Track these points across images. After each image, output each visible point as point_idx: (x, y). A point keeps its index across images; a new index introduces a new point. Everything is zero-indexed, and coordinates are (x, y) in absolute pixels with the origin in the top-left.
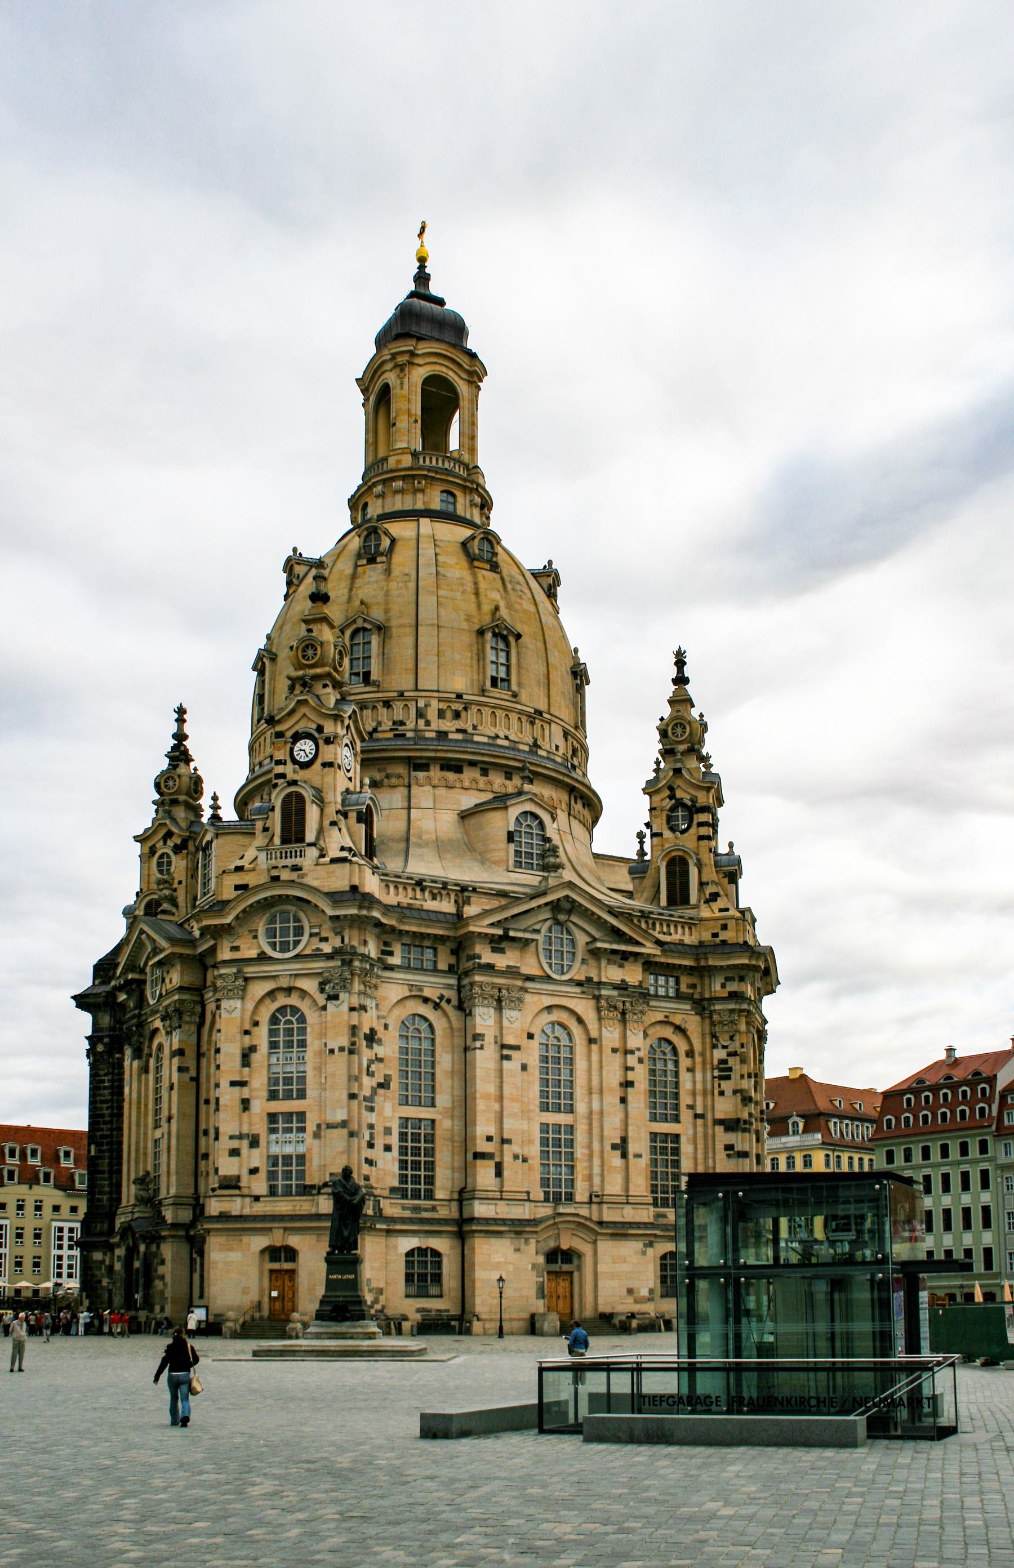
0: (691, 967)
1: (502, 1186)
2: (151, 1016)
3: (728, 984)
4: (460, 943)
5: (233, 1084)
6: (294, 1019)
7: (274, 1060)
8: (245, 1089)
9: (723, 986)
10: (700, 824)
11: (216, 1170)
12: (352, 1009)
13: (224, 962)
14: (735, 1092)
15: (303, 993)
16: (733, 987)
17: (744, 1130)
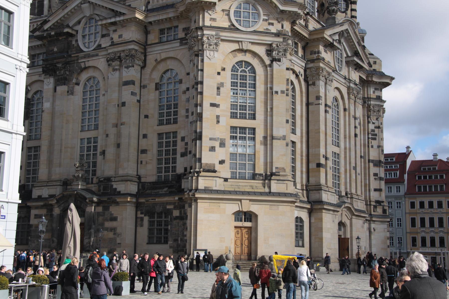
0: (364, 80)
1: (326, 184)
2: (84, 57)
3: (376, 91)
4: (307, 43)
5: (213, 105)
6: (247, 70)
7: (232, 93)
8: (217, 109)
9: (374, 92)
10: (352, 10)
11: (200, 160)
12: (288, 69)
13: (207, 27)
14: (379, 147)
15: (255, 54)
16: (377, 93)
17: (382, 167)
